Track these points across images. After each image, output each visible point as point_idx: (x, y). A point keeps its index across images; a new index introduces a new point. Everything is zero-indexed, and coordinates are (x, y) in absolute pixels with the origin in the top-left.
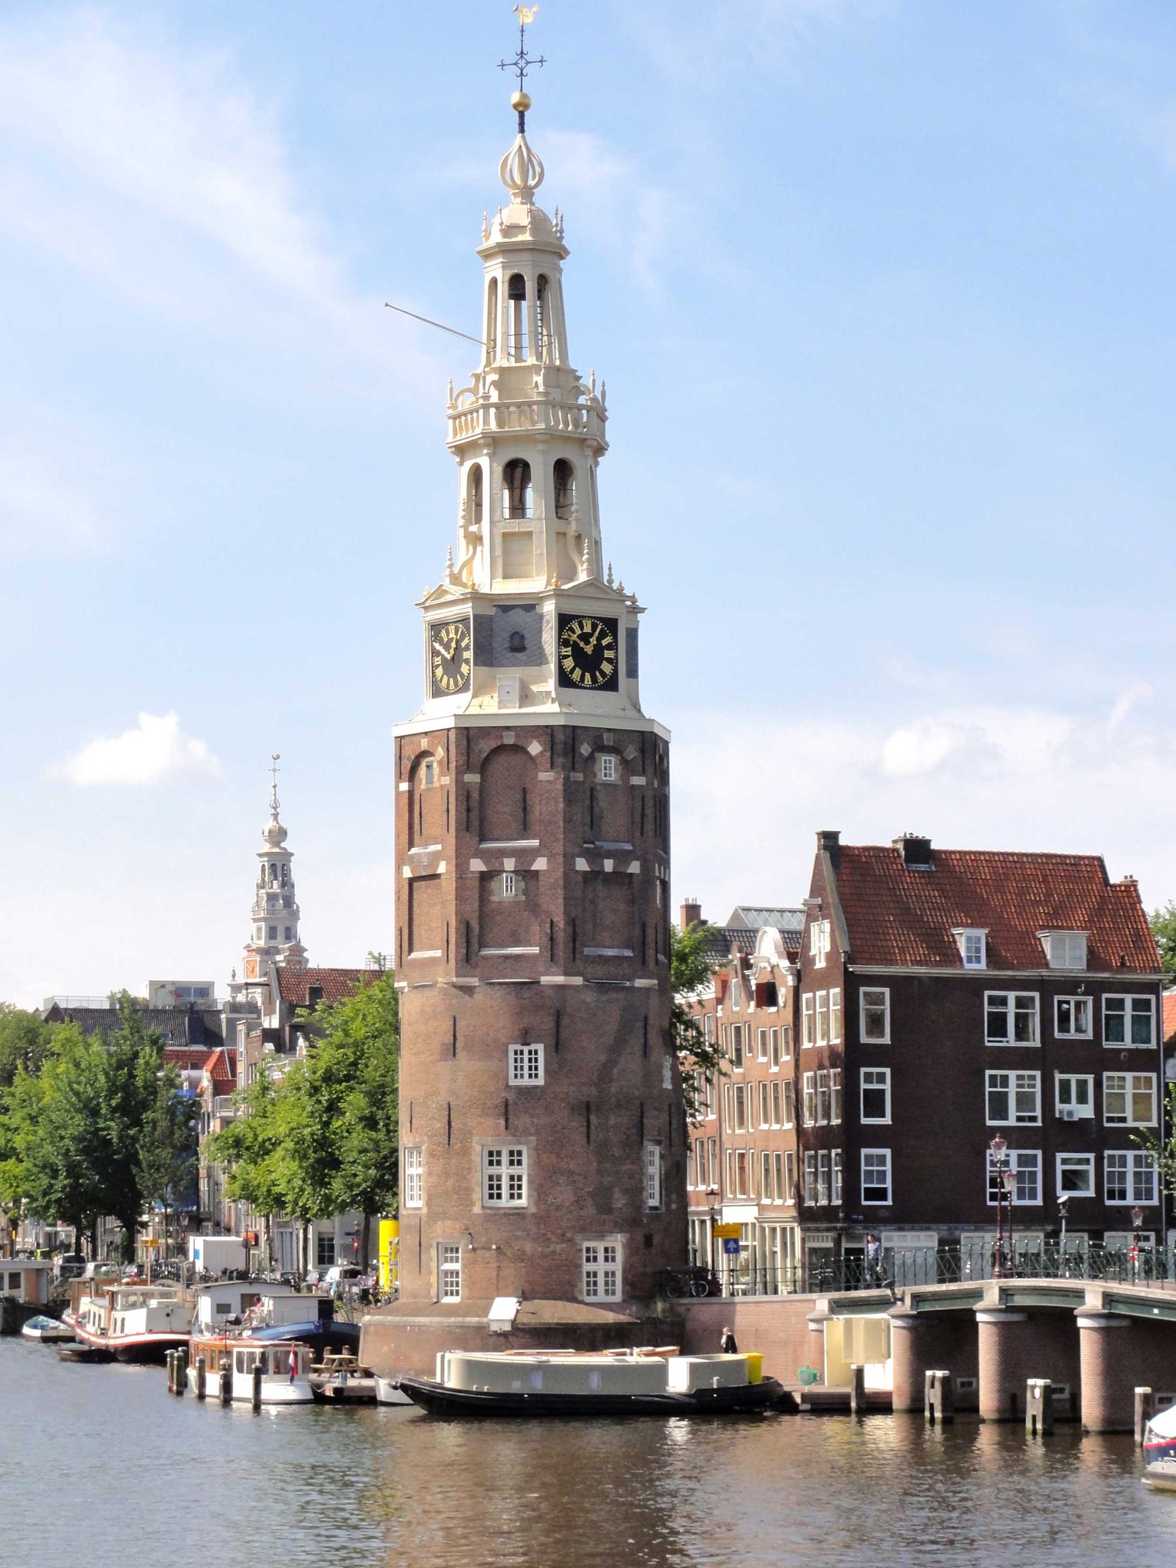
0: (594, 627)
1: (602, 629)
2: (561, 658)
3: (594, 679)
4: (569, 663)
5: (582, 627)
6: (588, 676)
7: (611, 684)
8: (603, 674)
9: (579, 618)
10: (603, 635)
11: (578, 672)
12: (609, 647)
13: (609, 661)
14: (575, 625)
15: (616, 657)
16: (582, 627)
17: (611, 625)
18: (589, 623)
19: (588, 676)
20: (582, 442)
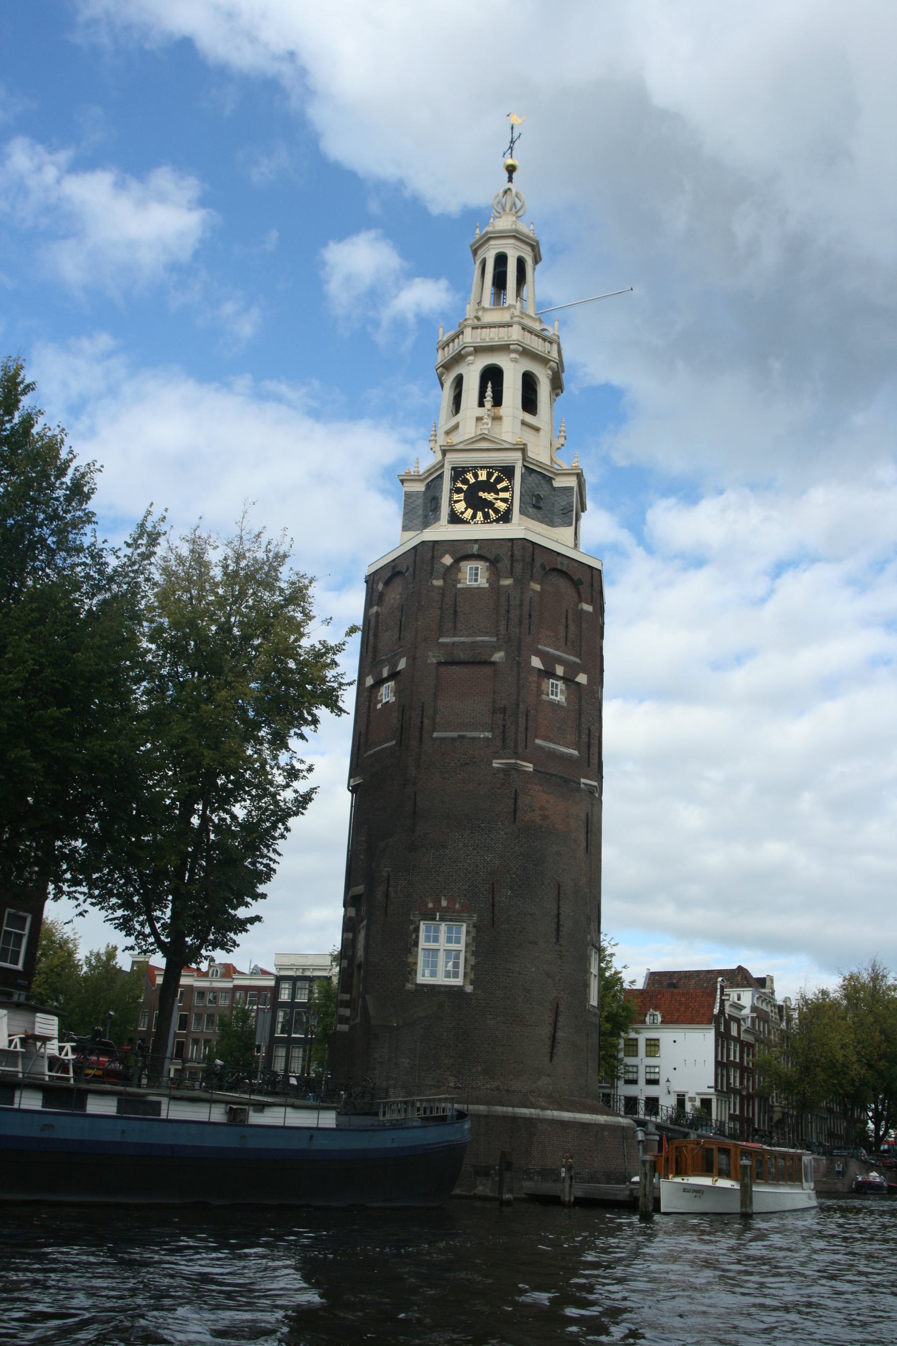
0: (489, 475)
1: (498, 477)
2: (452, 502)
3: (486, 516)
4: (460, 507)
5: (476, 476)
6: (480, 514)
7: (506, 518)
8: (496, 511)
9: (474, 470)
10: (499, 480)
11: (470, 512)
12: (505, 489)
13: (504, 500)
14: (470, 477)
15: (512, 497)
16: (476, 476)
17: (508, 472)
18: (484, 472)
19: (480, 514)
20: (504, 348)
